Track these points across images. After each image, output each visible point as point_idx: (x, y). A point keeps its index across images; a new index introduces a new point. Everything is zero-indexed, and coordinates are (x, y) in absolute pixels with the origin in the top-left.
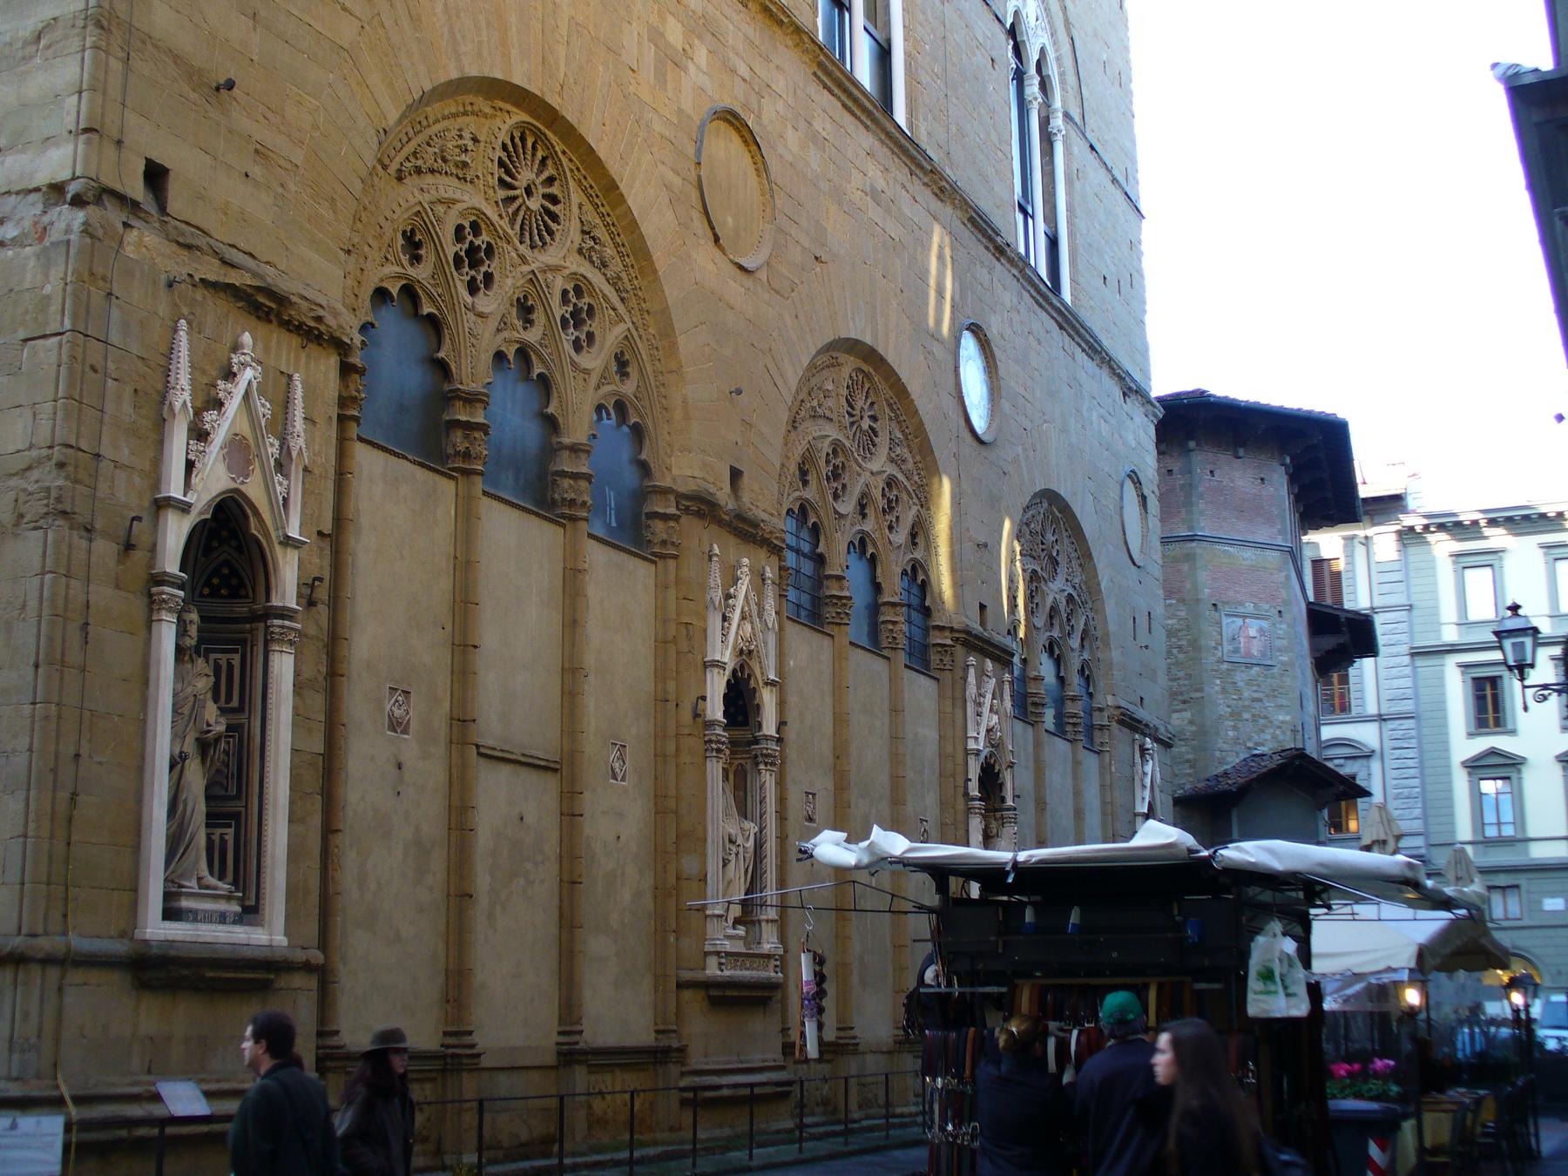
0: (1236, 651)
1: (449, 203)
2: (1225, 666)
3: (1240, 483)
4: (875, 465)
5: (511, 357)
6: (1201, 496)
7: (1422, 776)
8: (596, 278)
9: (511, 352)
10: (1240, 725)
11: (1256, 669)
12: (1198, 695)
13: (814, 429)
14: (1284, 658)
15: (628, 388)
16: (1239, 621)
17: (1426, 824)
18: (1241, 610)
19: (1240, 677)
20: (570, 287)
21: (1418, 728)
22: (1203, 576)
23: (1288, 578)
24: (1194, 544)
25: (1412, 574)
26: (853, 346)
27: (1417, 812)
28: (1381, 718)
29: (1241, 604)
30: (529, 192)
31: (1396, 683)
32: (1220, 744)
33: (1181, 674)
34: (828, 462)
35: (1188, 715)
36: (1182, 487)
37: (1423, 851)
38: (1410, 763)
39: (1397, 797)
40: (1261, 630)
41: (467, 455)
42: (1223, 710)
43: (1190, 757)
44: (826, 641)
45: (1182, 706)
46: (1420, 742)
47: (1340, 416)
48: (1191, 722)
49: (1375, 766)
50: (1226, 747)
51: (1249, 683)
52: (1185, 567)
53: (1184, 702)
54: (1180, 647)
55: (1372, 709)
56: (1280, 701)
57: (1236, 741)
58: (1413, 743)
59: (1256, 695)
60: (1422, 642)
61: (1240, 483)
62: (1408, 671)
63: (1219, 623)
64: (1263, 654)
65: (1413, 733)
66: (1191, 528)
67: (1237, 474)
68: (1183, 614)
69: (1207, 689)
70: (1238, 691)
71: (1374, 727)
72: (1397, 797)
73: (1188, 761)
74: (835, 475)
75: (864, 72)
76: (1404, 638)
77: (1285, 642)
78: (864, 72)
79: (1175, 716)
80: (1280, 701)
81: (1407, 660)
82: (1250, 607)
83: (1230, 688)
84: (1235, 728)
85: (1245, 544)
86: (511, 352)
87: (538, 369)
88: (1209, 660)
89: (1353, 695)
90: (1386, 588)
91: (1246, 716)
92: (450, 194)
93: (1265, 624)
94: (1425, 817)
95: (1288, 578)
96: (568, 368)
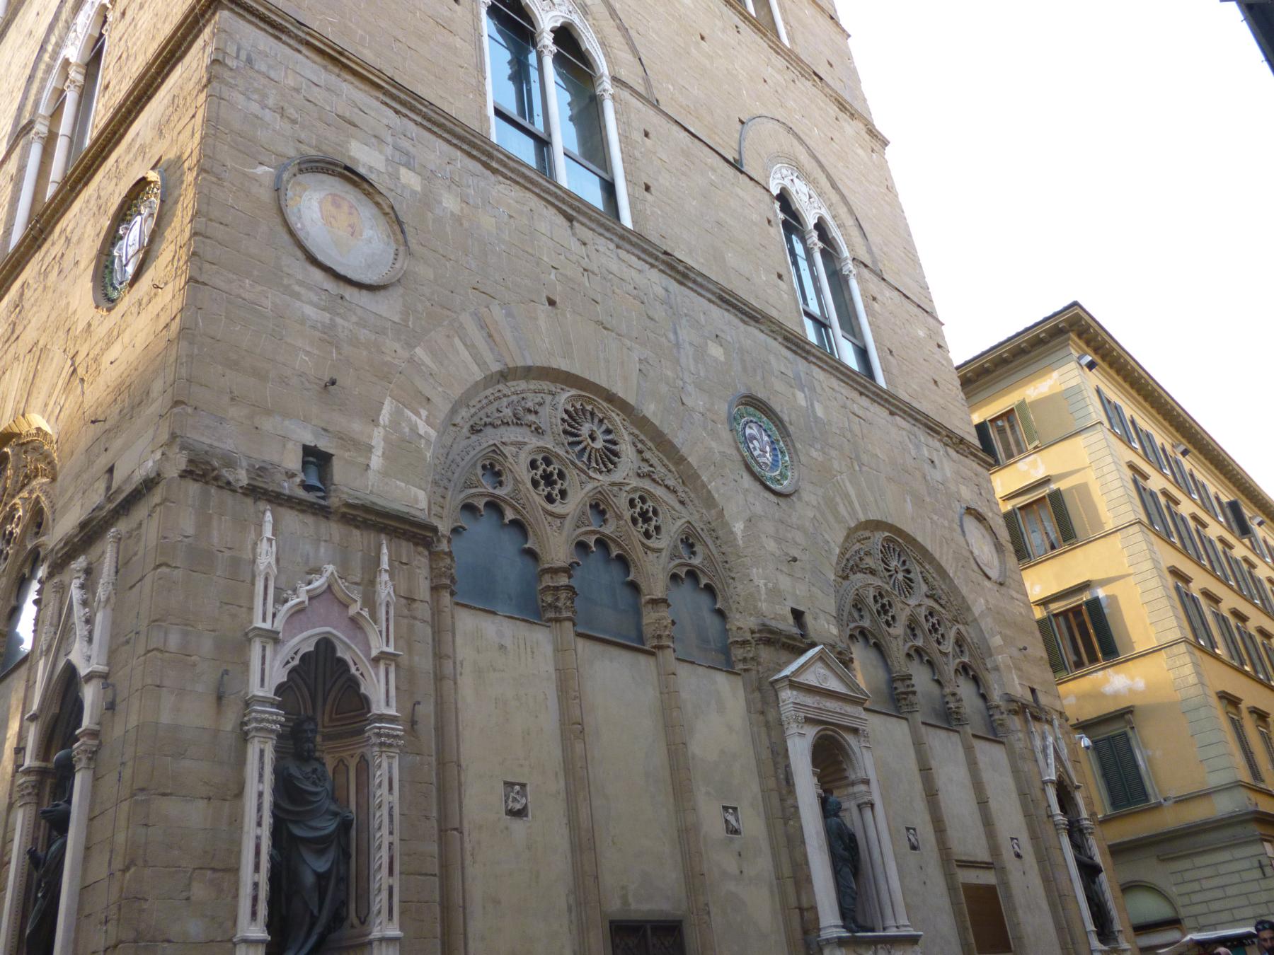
1: (519, 445)
4: (912, 602)
5: (592, 544)
8: (659, 492)
9: (591, 541)
13: (859, 579)
15: (696, 561)
20: (636, 496)
26: (877, 525)
30: (593, 438)
34: (876, 601)
41: (557, 609)
44: (904, 722)
74: (884, 609)
75: (849, 357)
78: (849, 357)
86: (591, 541)
87: (615, 552)
92: (520, 439)
96: (639, 548)
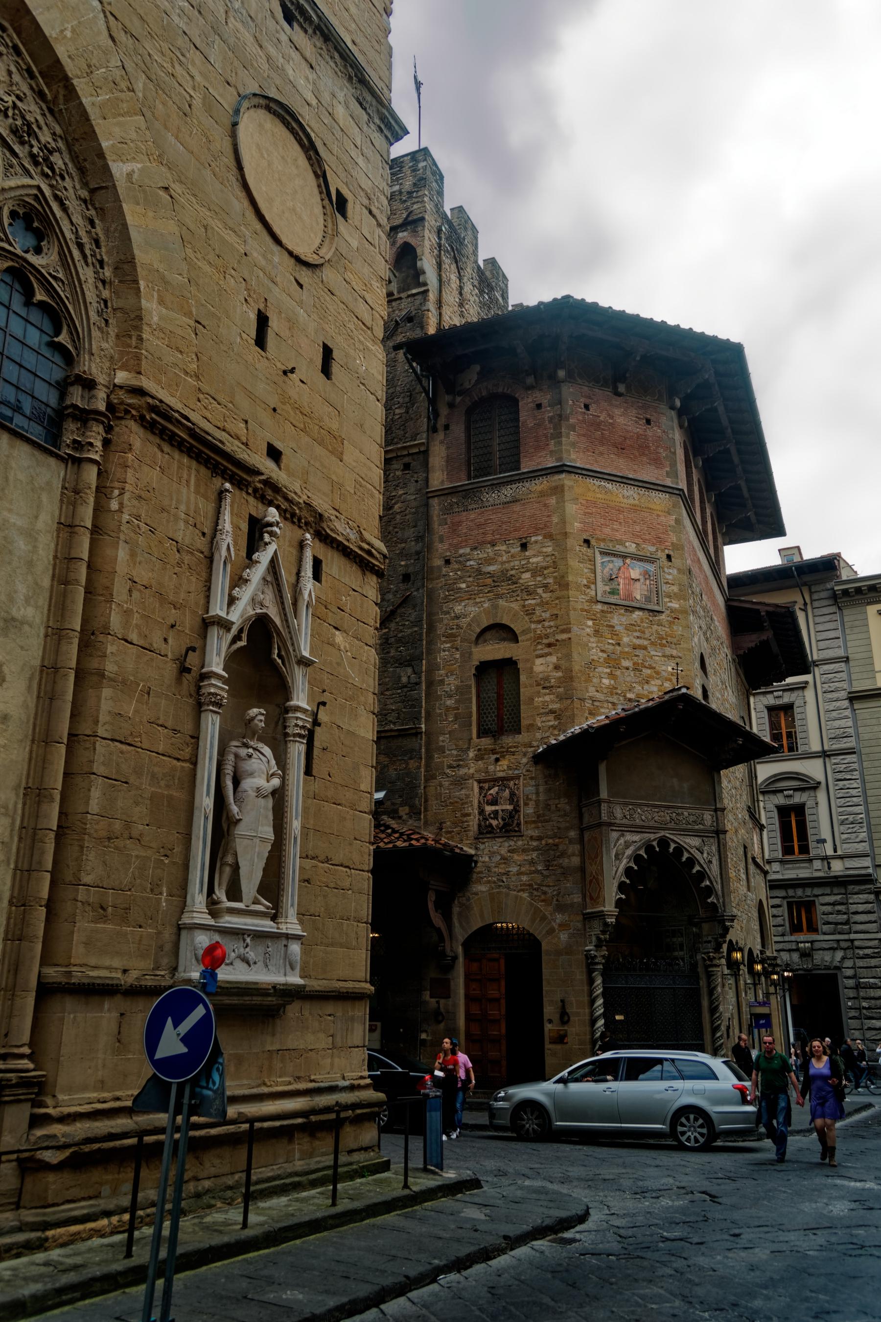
0: (614, 592)
2: (599, 607)
3: (621, 420)
6: (573, 428)
7: (866, 803)
10: (618, 673)
11: (638, 613)
12: (564, 636)
14: (675, 605)
16: (618, 562)
17: (872, 846)
18: (620, 548)
19: (618, 620)
21: (861, 761)
22: (571, 509)
23: (678, 521)
24: (563, 476)
25: (847, 631)
27: (863, 835)
28: (825, 755)
29: (621, 543)
31: (837, 724)
32: (592, 692)
33: (546, 615)
35: (553, 659)
36: (551, 419)
37: (870, 871)
38: (854, 792)
39: (842, 823)
40: (646, 574)
42: (596, 654)
43: (556, 706)
45: (547, 650)
46: (862, 775)
47: (734, 339)
48: (557, 668)
49: (821, 796)
50: (599, 696)
51: (630, 627)
52: (552, 501)
53: (549, 645)
54: (546, 586)
55: (816, 747)
56: (668, 651)
57: (612, 690)
58: (856, 774)
59: (638, 642)
60: (860, 685)
61: (621, 420)
62: (848, 713)
63: (593, 561)
64: (648, 599)
65: (855, 766)
66: (558, 460)
67: (617, 412)
68: (550, 549)
69: (575, 629)
70: (614, 634)
71: (819, 762)
72: (842, 823)
73: (552, 712)
76: (845, 685)
77: (675, 589)
79: (539, 661)
80: (668, 651)
81: (846, 703)
82: (631, 548)
83: (605, 631)
84: (611, 675)
85: (624, 480)
88: (578, 599)
89: (799, 736)
90: (822, 645)
91: (626, 663)
93: (651, 568)
94: (871, 839)
95: (678, 521)
